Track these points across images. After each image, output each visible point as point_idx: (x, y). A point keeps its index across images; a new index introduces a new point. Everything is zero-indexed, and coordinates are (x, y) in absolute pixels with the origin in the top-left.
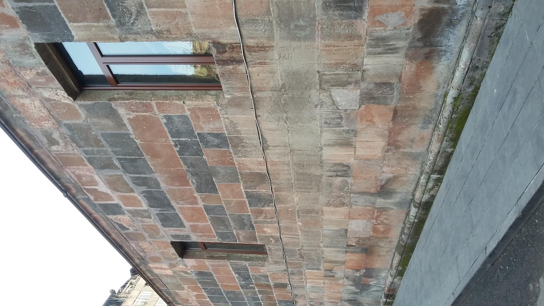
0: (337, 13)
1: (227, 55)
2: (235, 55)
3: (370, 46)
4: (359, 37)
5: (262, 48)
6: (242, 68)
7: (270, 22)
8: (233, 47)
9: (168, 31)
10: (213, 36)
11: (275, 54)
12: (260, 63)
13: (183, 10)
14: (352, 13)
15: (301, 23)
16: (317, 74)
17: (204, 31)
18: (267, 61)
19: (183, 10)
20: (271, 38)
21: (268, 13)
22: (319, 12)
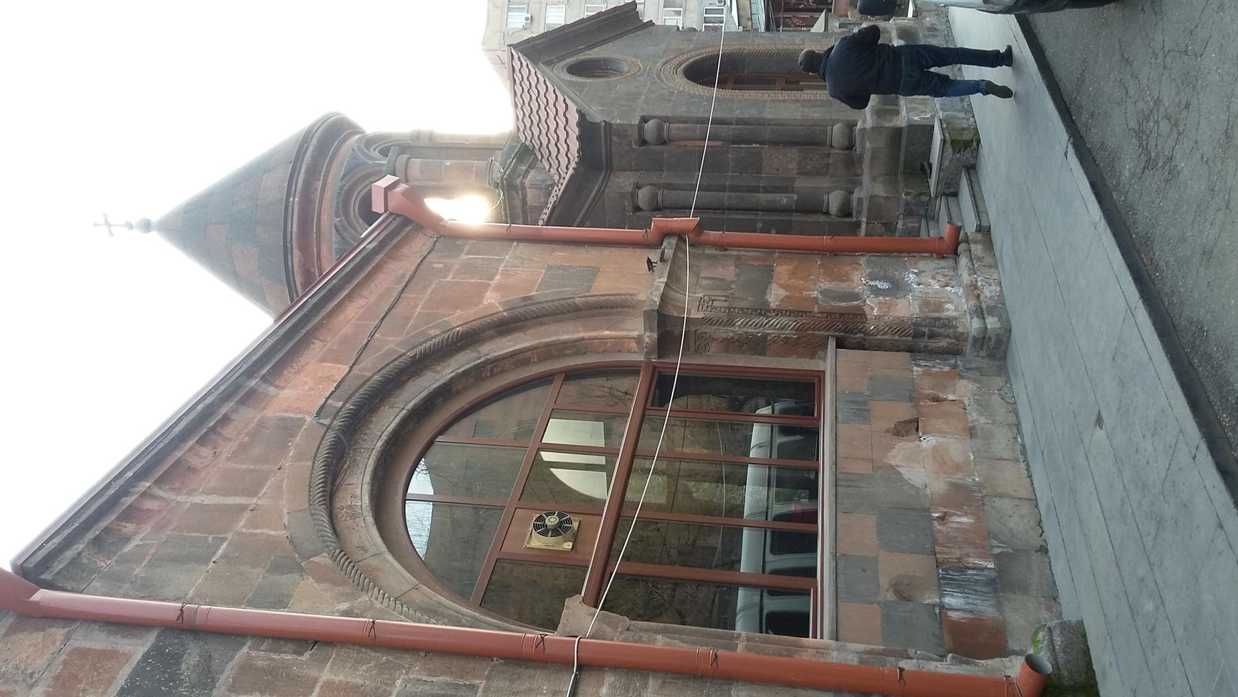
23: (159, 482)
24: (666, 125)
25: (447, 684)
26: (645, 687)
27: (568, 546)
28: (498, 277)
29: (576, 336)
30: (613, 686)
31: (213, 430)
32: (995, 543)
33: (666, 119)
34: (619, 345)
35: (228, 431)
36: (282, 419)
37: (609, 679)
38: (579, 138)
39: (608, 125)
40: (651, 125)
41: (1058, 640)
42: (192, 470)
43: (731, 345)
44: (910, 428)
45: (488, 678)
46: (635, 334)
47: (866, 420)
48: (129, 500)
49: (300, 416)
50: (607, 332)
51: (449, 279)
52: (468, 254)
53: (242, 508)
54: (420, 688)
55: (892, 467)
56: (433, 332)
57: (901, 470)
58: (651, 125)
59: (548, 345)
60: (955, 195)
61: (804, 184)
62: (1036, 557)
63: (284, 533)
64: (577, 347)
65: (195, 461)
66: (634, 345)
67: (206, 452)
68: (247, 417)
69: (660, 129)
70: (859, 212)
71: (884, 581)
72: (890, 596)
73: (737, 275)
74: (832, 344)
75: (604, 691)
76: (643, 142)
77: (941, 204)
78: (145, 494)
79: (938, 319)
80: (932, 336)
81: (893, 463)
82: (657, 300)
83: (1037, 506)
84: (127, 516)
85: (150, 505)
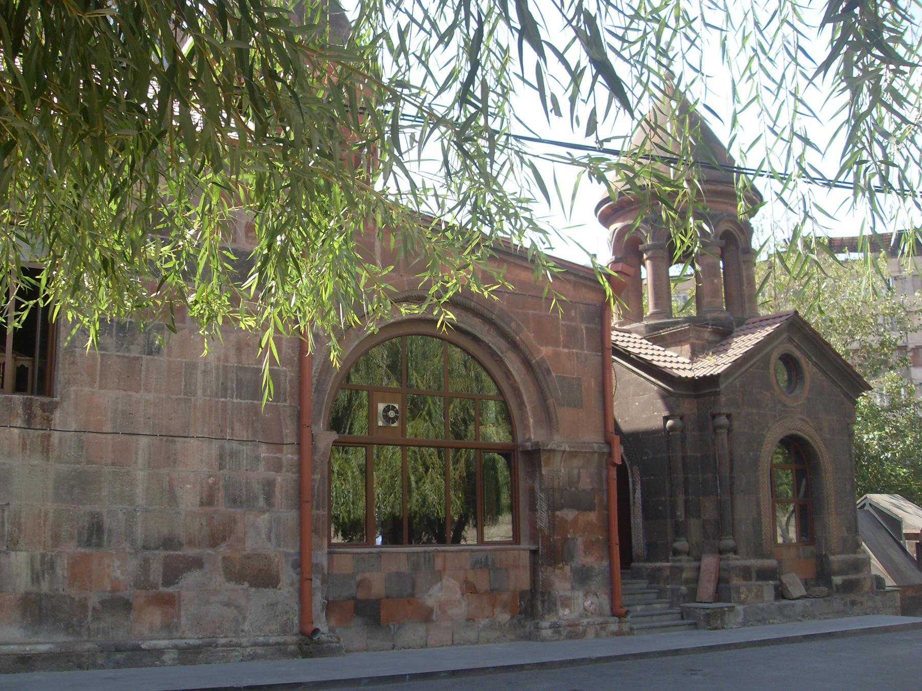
0: (86, 524)
1: (39, 412)
2: (38, 420)
3: (43, 556)
4: (55, 545)
5: (46, 449)
6: (19, 422)
7: (79, 463)
8: (49, 420)
9: (73, 363)
10: (65, 405)
11: (37, 460)
12: (24, 444)
13: (97, 385)
14: (85, 538)
15: (76, 491)
16: (4, 503)
17: (73, 396)
18: (28, 452)
19: (97, 385)
20: (59, 459)
21: (89, 462)
22: (88, 508)
24: (725, 431)
25: (286, 390)
26: (293, 473)
27: (380, 424)
28: (566, 350)
29: (527, 404)
30: (292, 459)
32: (397, 626)
33: (729, 430)
34: (526, 428)
37: (296, 457)
38: (705, 376)
39: (717, 394)
40: (723, 420)
41: (334, 645)
43: (532, 491)
44: (470, 589)
45: (290, 406)
46: (532, 437)
47: (473, 568)
50: (531, 421)
52: (586, 328)
54: (282, 378)
55: (441, 580)
56: (513, 325)
57: (439, 584)
58: (723, 420)
59: (519, 388)
60: (682, 618)
61: (694, 525)
62: (390, 644)
64: (521, 405)
66: (527, 437)
69: (721, 427)
70: (674, 561)
71: (367, 575)
72: (359, 577)
73: (584, 491)
74: (533, 547)
75: (290, 456)
76: (714, 417)
77: (677, 610)
79: (555, 605)
80: (543, 602)
81: (444, 581)
82: (549, 447)
83: (422, 647)
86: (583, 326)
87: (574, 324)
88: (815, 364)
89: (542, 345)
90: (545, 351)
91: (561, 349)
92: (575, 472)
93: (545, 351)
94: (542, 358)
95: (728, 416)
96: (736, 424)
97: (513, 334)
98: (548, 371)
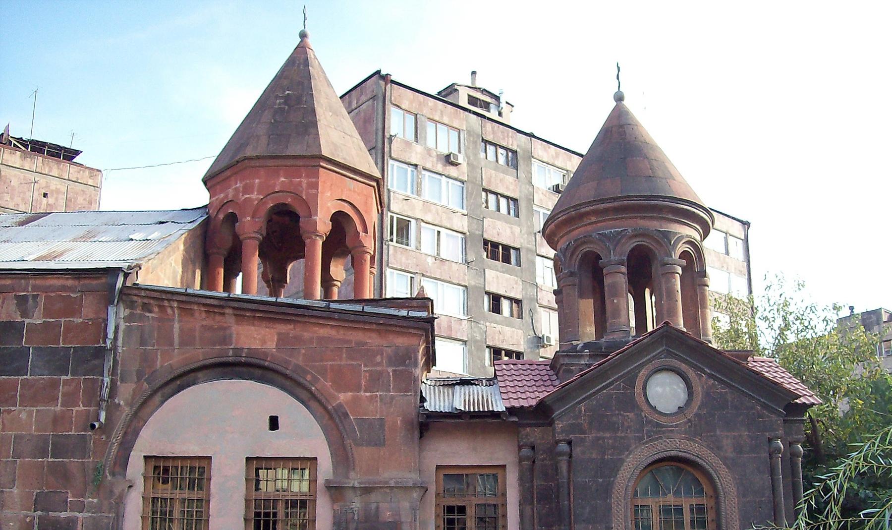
23: (179, 308)
28: (368, 394)
31: (215, 313)
35: (218, 318)
36: (231, 336)
42: (192, 315)
48: (166, 303)
49: (234, 341)
51: (363, 369)
52: (394, 371)
53: (172, 344)
58: (563, 447)
63: (159, 366)
65: (197, 314)
67: (204, 315)
68: (230, 320)
69: (561, 454)
78: (172, 307)
84: (160, 306)
85: (169, 311)
86: (390, 370)
87: (379, 369)
88: (710, 376)
89: (340, 392)
90: (343, 397)
91: (362, 393)
92: (374, 506)
93: (343, 397)
94: (340, 405)
95: (569, 443)
96: (577, 451)
97: (308, 384)
98: (346, 415)
